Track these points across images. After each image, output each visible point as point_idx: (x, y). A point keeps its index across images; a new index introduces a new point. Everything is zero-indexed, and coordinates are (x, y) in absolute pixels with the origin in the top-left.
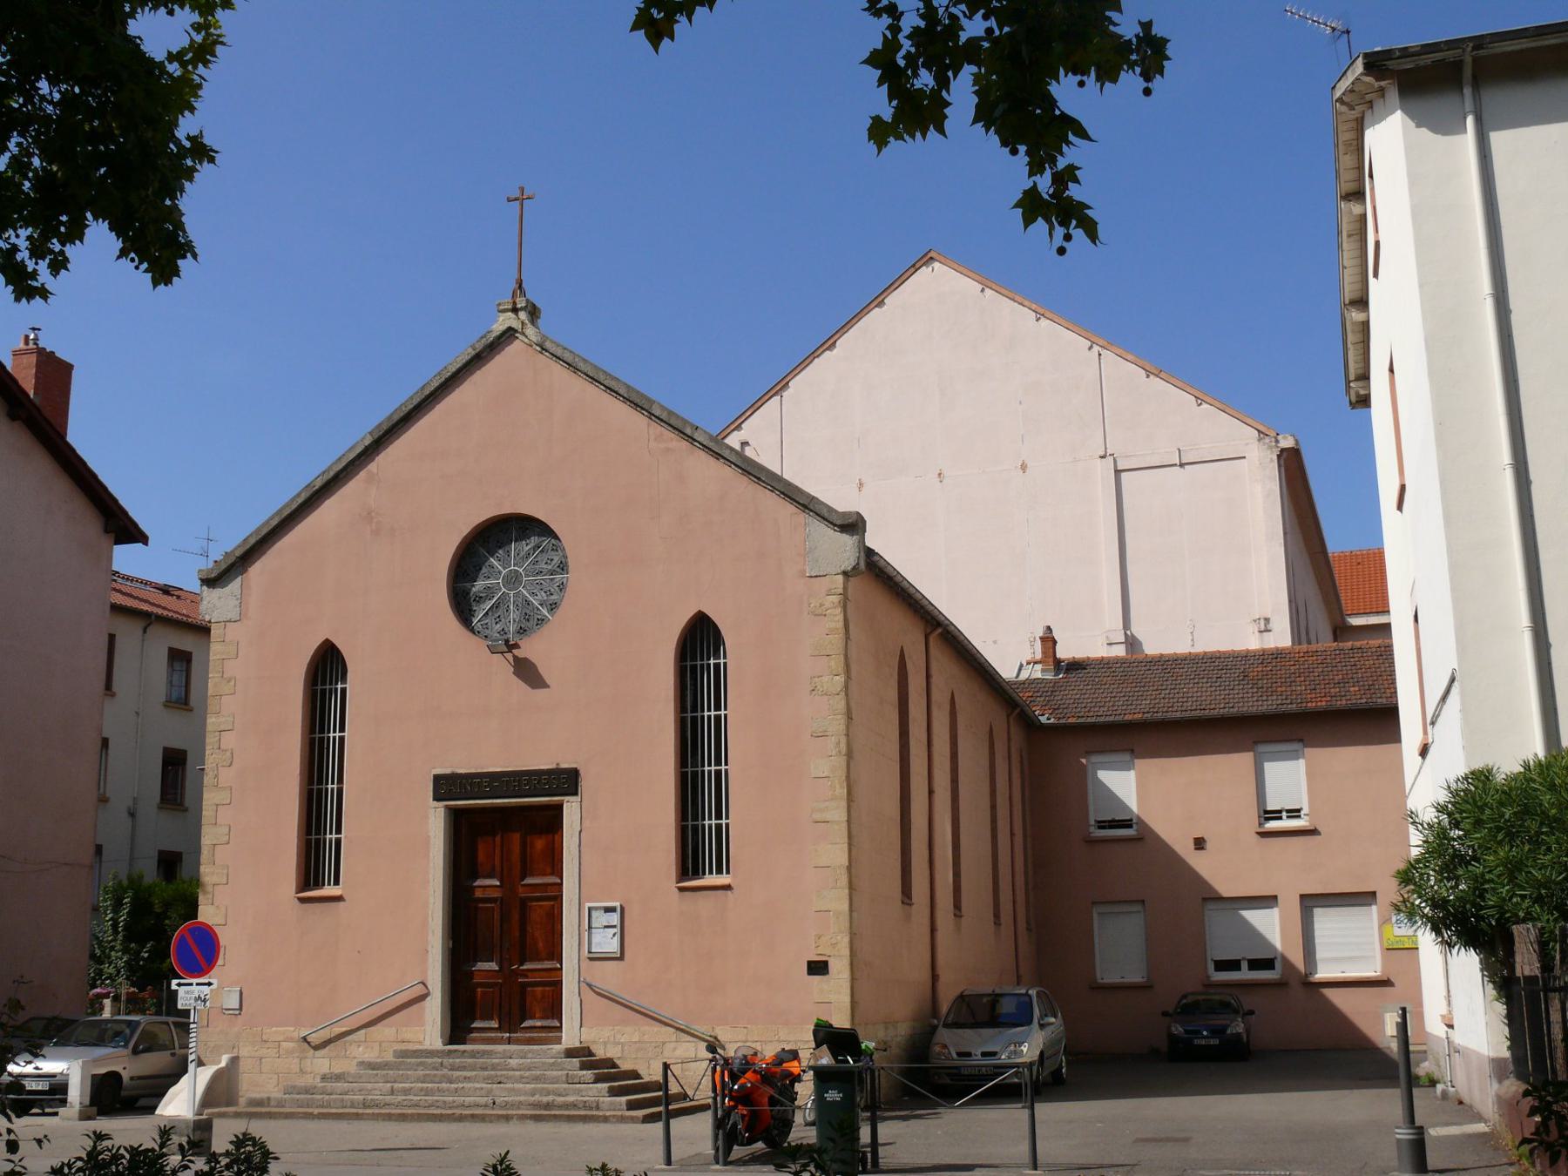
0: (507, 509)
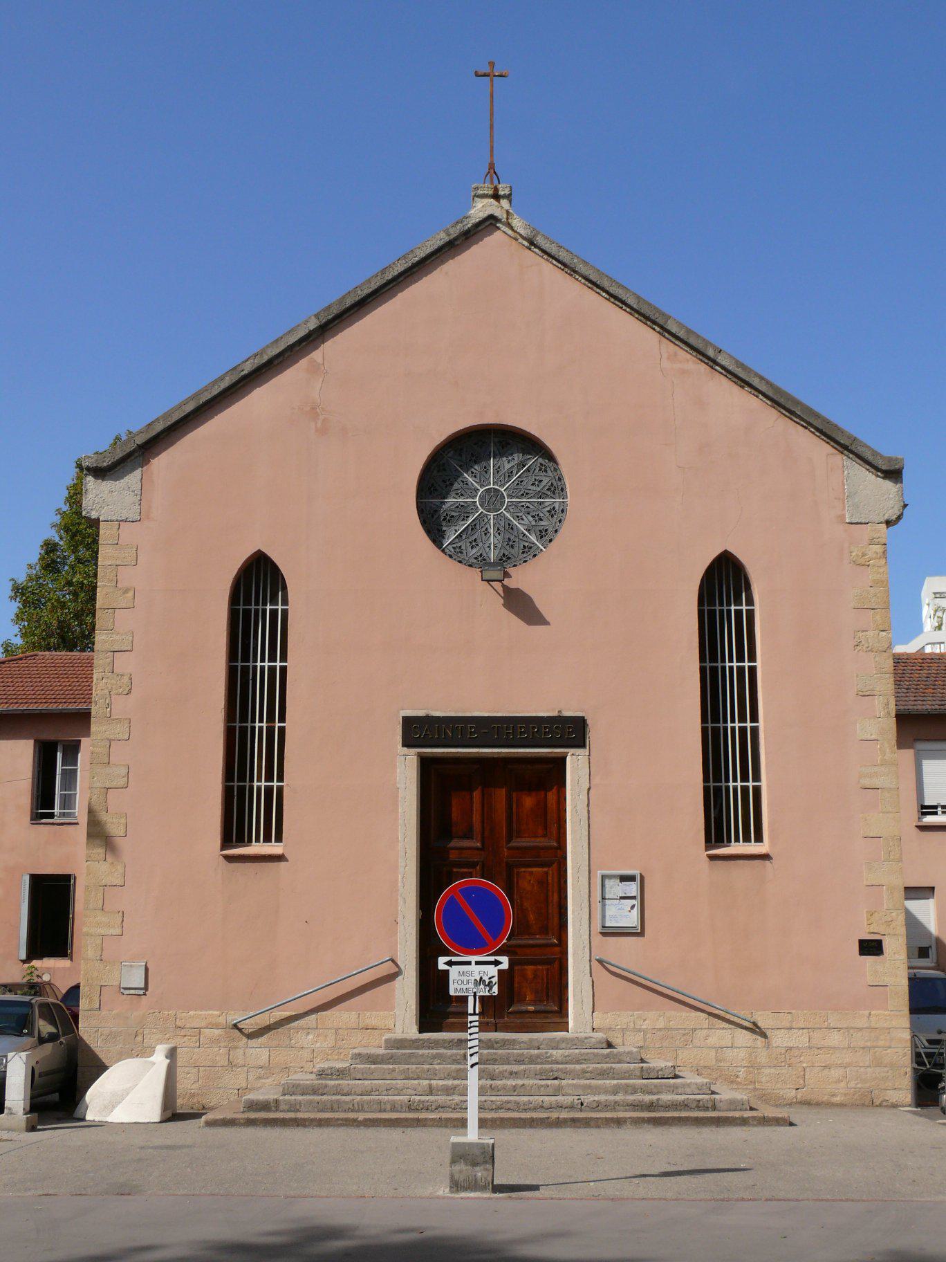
0: (490, 419)
